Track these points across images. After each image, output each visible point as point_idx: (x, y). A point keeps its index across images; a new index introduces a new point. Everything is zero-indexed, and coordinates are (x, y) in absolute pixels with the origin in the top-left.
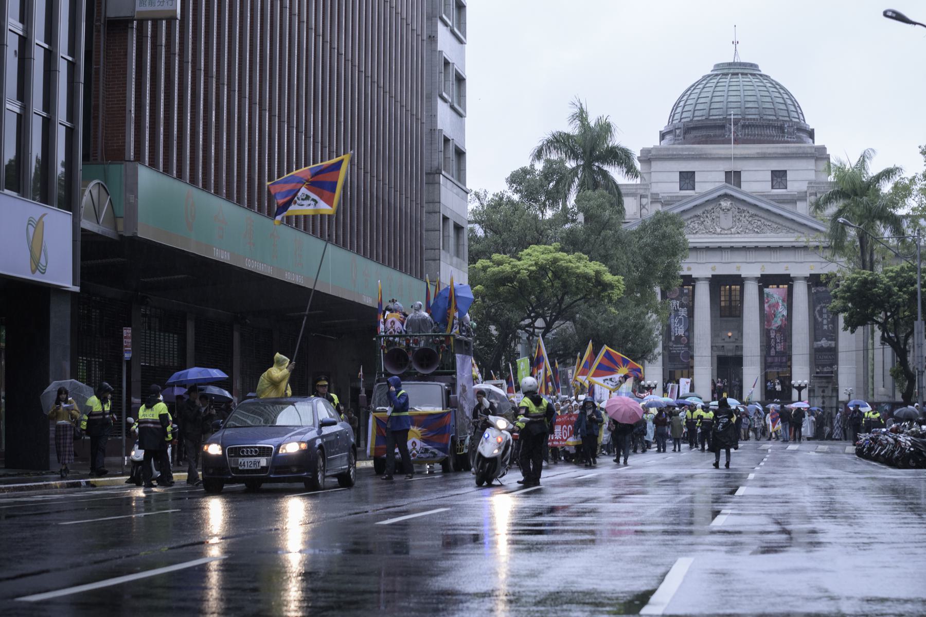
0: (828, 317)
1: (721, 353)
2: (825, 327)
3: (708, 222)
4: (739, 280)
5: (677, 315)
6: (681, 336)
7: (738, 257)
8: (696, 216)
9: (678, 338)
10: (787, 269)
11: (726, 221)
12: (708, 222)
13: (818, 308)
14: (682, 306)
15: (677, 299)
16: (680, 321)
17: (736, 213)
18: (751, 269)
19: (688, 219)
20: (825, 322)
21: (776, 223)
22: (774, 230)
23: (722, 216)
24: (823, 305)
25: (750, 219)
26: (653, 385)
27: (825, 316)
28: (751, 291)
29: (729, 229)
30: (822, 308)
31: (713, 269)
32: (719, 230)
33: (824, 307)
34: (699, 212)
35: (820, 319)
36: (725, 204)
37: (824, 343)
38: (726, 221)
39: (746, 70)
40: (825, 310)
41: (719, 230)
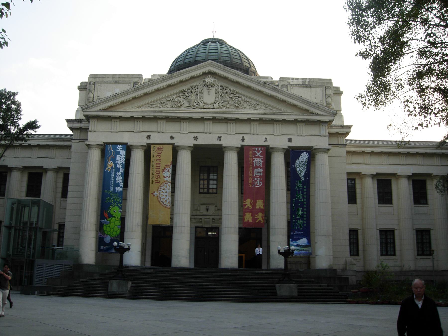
1: (200, 225)
7: (220, 128)
8: (183, 91)
10: (266, 140)
11: (209, 97)
12: (192, 97)
17: (219, 90)
18: (231, 138)
19: (174, 94)
21: (255, 100)
22: (253, 106)
25: (232, 96)
26: (127, 247)
28: (231, 162)
31: (196, 138)
32: (202, 105)
34: (185, 88)
36: (209, 80)
39: (221, 42)
41: (202, 105)
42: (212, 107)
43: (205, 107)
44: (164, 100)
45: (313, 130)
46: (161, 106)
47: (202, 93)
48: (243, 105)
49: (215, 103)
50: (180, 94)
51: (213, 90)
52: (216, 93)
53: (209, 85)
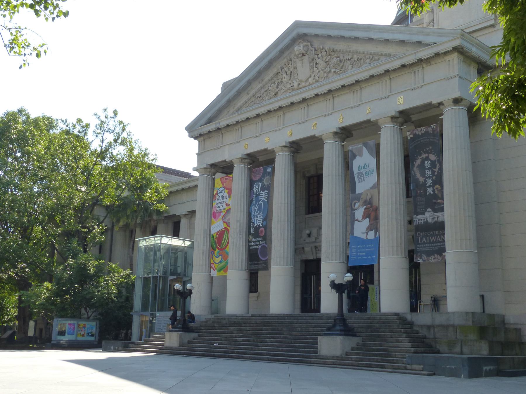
0: (433, 172)
2: (430, 191)
3: (285, 78)
4: (315, 143)
5: (258, 200)
6: (259, 227)
9: (257, 229)
13: (418, 162)
14: (263, 188)
15: (260, 180)
16: (259, 209)
18: (323, 123)
20: (429, 182)
24: (424, 156)
27: (429, 173)
29: (307, 80)
30: (423, 161)
33: (427, 159)
35: (421, 179)
37: (429, 216)
40: (428, 164)
42: (307, 84)
43: (300, 86)
45: (431, 73)
46: (258, 102)
47: (296, 68)
48: (342, 67)
49: (310, 77)
50: (275, 79)
51: (306, 57)
52: (310, 63)
53: (300, 54)
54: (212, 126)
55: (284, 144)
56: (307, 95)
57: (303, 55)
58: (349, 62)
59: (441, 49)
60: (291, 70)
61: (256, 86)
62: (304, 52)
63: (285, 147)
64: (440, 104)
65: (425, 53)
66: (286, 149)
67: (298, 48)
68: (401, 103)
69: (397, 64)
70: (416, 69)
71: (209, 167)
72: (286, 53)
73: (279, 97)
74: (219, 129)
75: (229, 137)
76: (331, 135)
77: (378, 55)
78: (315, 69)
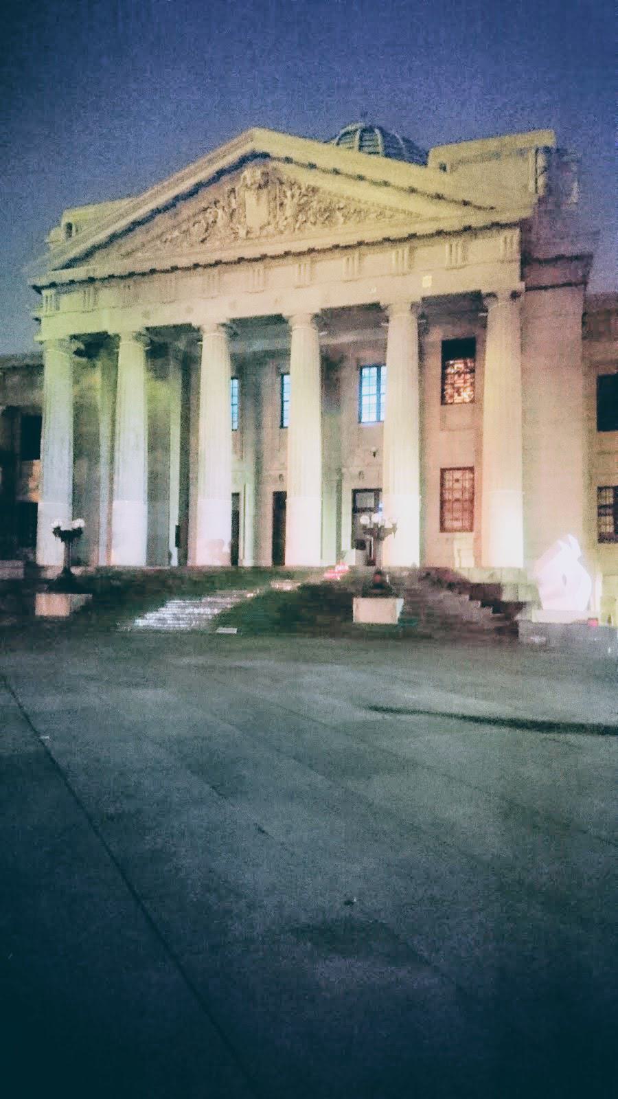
23: (250, 197)
38: (255, 208)
44: (176, 233)
47: (243, 205)
54: (79, 273)
55: (224, 321)
56: (271, 250)
57: (260, 187)
58: (338, 214)
59: (503, 218)
60: (234, 206)
61: (163, 221)
62: (262, 183)
63: (224, 325)
64: (492, 295)
65: (477, 219)
66: (223, 329)
67: (251, 174)
68: (429, 284)
69: (430, 228)
70: (455, 241)
71: (68, 339)
72: (225, 178)
73: (208, 244)
74: (91, 280)
75: (108, 295)
76: (309, 318)
77: (391, 209)
78: (278, 212)
